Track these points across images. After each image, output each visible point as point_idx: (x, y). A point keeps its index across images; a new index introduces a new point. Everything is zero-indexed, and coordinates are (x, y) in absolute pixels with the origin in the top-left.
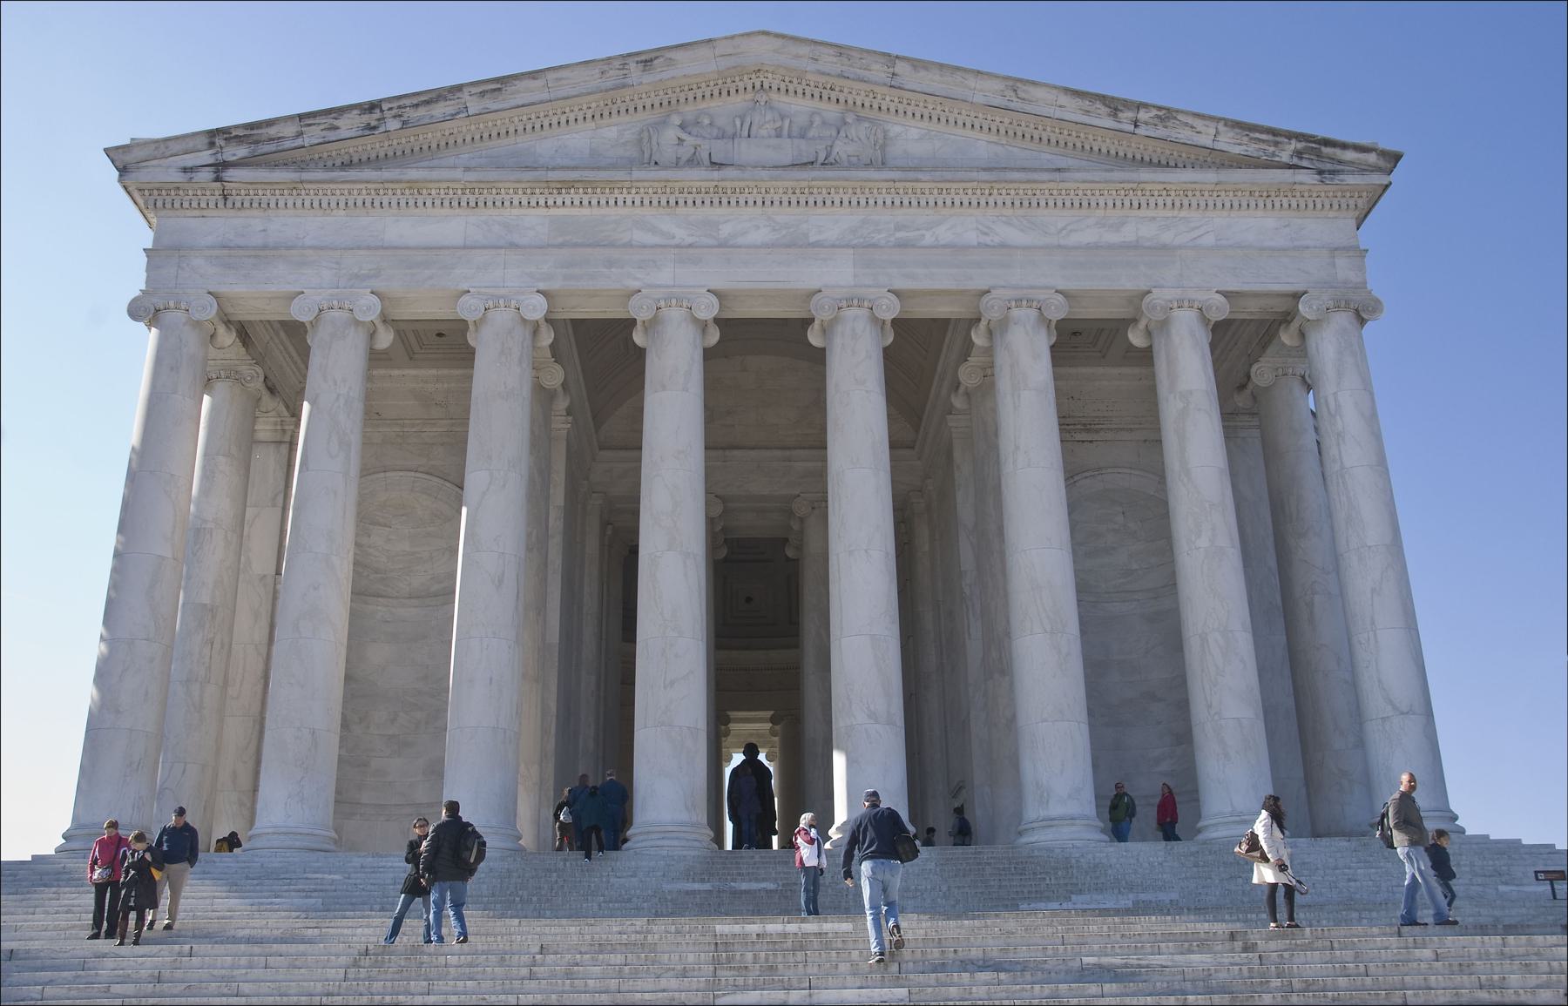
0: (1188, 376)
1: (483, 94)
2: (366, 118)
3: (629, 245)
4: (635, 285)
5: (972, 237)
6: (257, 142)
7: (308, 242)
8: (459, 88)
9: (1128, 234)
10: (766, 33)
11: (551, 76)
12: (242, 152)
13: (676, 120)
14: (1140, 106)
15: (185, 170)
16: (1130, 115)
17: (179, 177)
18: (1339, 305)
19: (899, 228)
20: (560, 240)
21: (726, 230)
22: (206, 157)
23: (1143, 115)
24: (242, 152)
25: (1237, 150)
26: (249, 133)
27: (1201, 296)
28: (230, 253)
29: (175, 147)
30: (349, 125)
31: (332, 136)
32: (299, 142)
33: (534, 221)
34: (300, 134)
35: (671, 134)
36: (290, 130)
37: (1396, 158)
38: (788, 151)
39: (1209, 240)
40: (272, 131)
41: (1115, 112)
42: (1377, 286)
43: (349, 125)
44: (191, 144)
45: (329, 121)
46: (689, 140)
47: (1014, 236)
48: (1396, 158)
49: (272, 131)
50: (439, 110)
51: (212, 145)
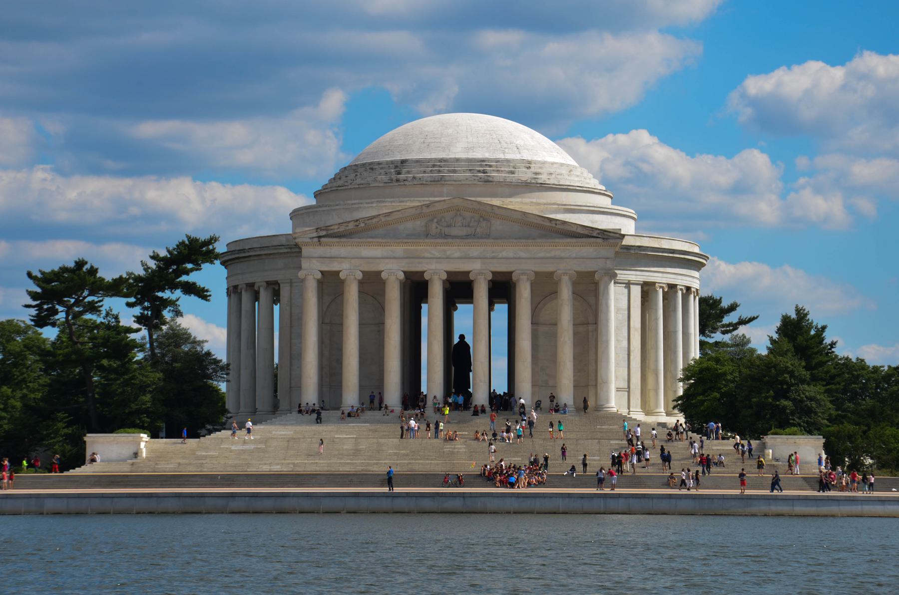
0: (566, 293)
3: (424, 258)
4: (425, 269)
5: (511, 255)
9: (553, 254)
12: (324, 233)
13: (435, 220)
21: (448, 253)
22: (315, 235)
26: (327, 228)
33: (399, 250)
35: (434, 225)
36: (336, 227)
38: (463, 231)
39: (574, 255)
46: (439, 227)
47: (523, 254)
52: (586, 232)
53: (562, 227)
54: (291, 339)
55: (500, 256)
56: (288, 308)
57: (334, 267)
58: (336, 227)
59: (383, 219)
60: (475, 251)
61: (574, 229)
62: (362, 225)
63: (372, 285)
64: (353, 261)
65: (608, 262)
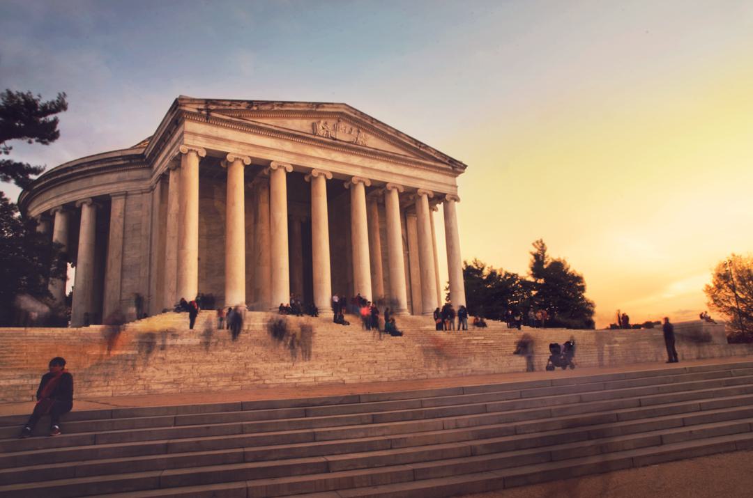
1: (278, 105)
2: (248, 105)
6: (219, 105)
7: (229, 138)
8: (273, 102)
10: (345, 105)
11: (295, 104)
14: (422, 143)
15: (198, 109)
16: (419, 144)
17: (196, 111)
18: (452, 199)
19: (370, 162)
20: (294, 151)
22: (202, 107)
23: (422, 146)
24: (214, 107)
25: (438, 158)
27: (428, 192)
28: (207, 137)
29: (196, 102)
30: (243, 107)
31: (239, 108)
32: (229, 108)
34: (230, 105)
36: (228, 103)
37: (465, 166)
40: (224, 103)
41: (416, 144)
42: (460, 194)
43: (243, 107)
44: (200, 102)
45: (239, 103)
48: (465, 166)
49: (224, 103)
50: (267, 107)
51: (206, 103)
52: (441, 159)
53: (424, 150)
54: (123, 251)
55: (375, 168)
56: (121, 220)
57: (222, 147)
58: (228, 103)
59: (276, 108)
60: (356, 160)
61: (433, 154)
62: (255, 108)
63: (258, 174)
64: (242, 146)
65: (454, 188)
